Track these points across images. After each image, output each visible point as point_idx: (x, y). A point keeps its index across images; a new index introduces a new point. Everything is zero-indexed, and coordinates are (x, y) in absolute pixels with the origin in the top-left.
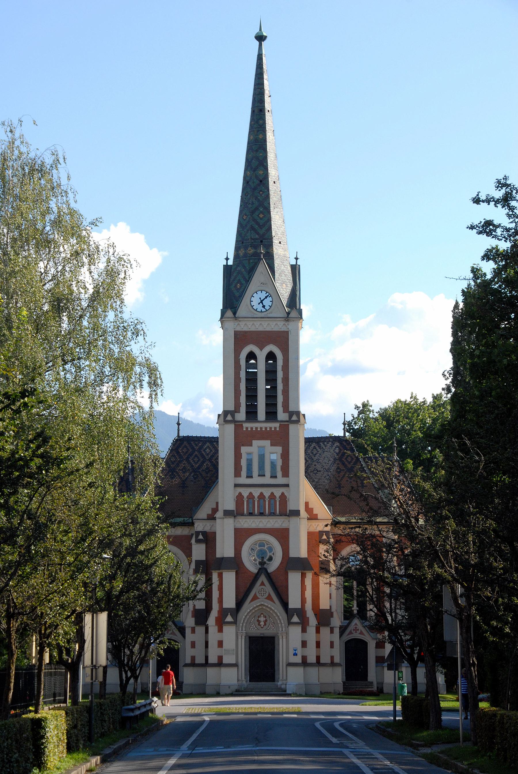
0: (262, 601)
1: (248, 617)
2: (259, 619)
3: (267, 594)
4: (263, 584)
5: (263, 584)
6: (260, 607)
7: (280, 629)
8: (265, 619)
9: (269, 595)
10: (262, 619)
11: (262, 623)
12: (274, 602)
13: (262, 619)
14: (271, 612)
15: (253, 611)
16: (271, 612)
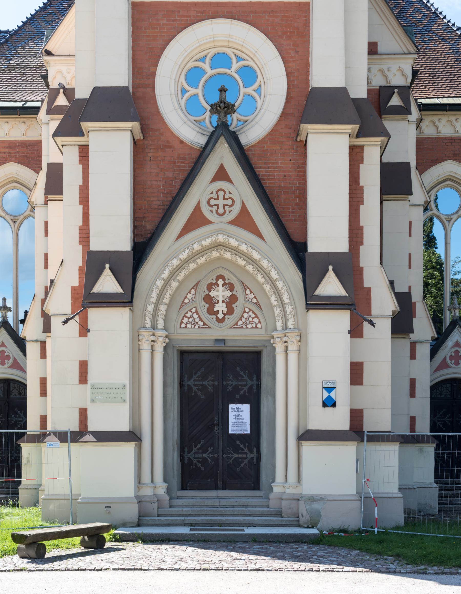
2: (212, 294)
8: (229, 293)
9: (244, 210)
10: (220, 293)
11: (221, 307)
13: (220, 293)
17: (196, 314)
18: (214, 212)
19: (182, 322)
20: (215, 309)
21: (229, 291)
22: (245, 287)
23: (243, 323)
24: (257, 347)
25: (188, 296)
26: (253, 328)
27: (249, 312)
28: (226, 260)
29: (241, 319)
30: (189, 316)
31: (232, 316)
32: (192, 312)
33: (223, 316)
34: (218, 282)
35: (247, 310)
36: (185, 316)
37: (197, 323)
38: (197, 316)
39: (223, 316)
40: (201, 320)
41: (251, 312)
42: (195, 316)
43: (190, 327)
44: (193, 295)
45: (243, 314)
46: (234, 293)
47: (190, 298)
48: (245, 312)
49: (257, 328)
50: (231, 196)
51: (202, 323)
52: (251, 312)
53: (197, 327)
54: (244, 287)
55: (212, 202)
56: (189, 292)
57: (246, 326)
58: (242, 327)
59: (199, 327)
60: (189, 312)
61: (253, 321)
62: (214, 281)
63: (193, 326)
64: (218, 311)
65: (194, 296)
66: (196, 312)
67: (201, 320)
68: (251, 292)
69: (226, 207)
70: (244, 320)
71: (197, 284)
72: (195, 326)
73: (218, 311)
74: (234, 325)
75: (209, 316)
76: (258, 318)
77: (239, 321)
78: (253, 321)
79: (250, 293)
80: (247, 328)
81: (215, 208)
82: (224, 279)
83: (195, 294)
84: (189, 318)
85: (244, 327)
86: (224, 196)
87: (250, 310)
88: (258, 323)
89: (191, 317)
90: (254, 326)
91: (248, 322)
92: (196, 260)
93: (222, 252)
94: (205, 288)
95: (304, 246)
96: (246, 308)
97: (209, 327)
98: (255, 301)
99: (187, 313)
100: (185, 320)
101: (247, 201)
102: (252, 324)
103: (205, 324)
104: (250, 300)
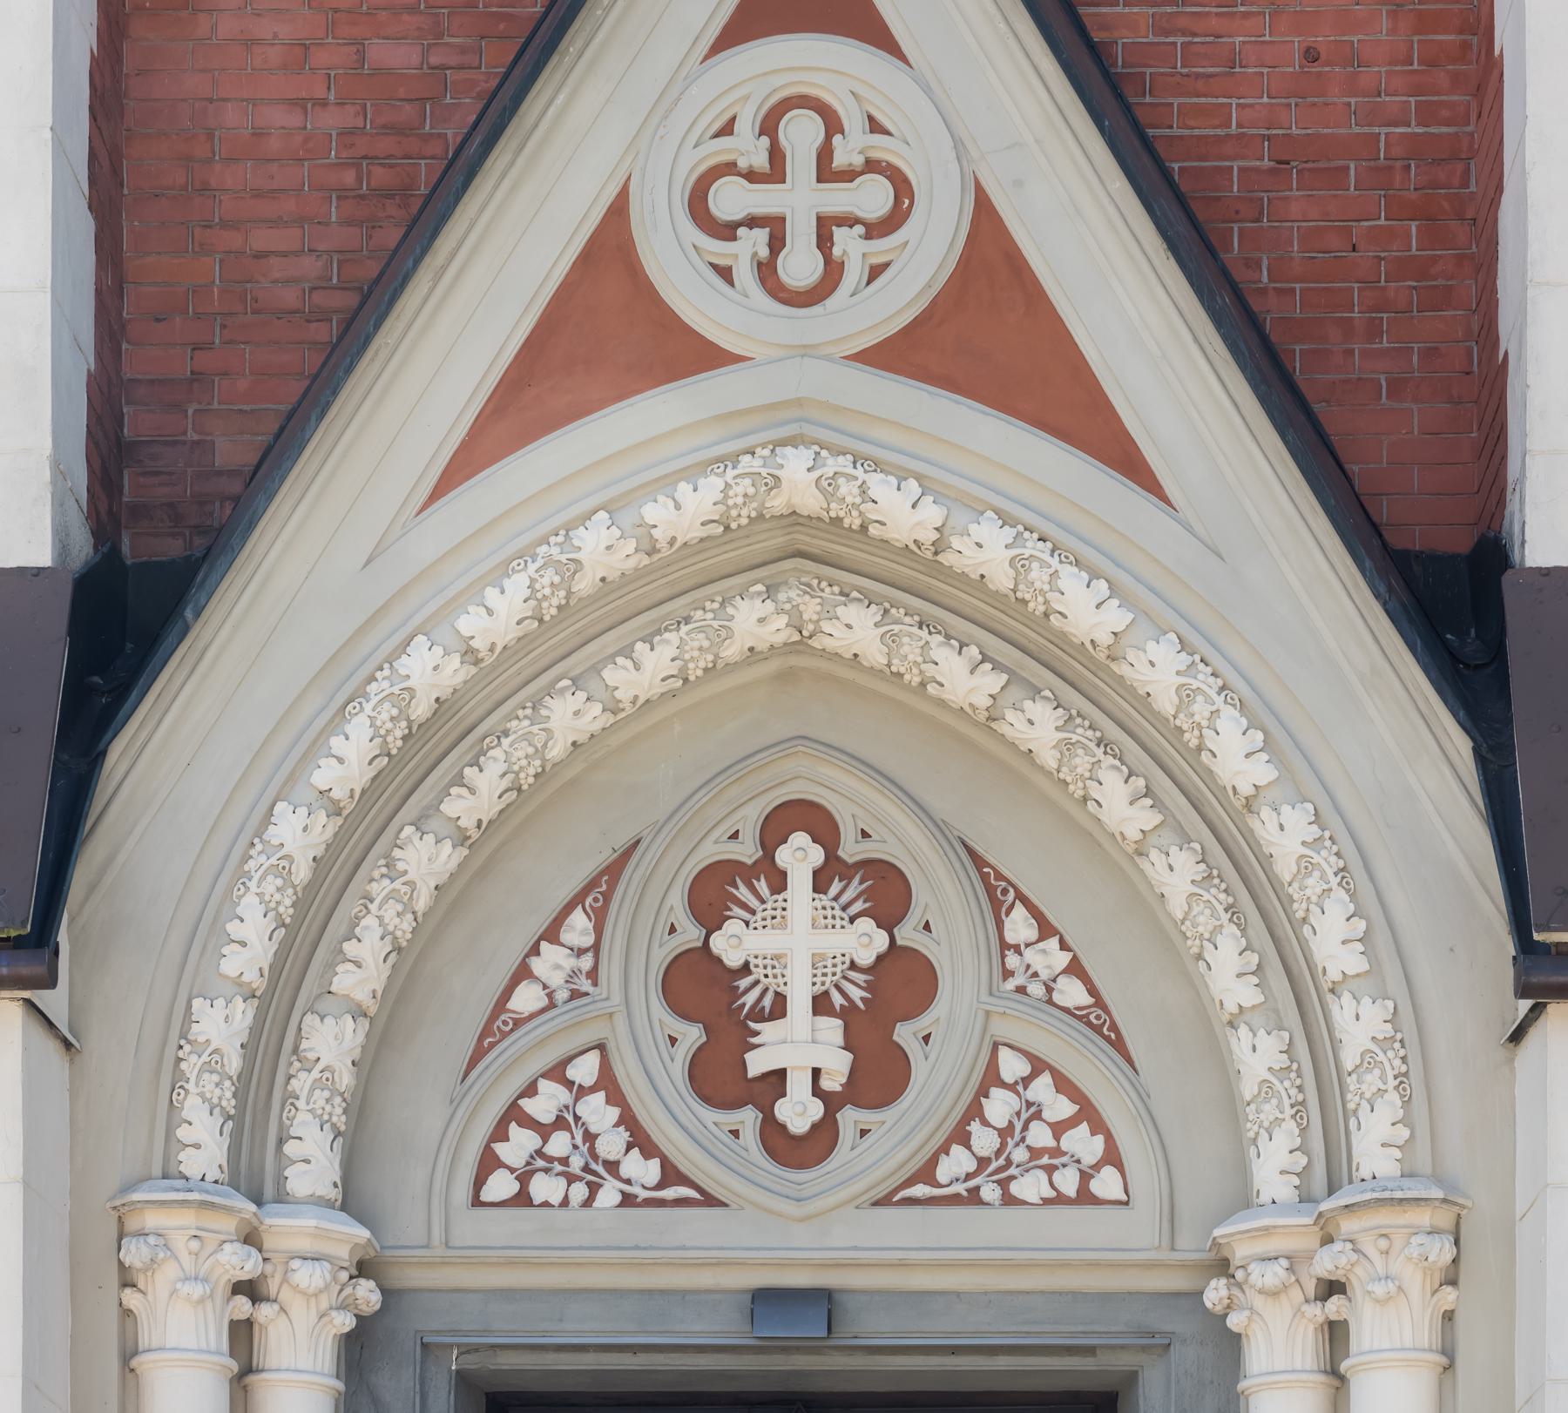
0: (794, 425)
1: (425, 860)
2: (731, 944)
3: (928, 252)
6: (754, 622)
7: (1275, 1164)
8: (866, 941)
9: (992, 262)
10: (799, 941)
11: (803, 1048)
12: (1127, 461)
13: (799, 941)
14: (1037, 726)
16: (1037, 726)
17: (600, 1097)
18: (745, 274)
19: (489, 1163)
20: (757, 1064)
21: (866, 924)
22: (997, 893)
23: (983, 1162)
24: (1090, 1350)
25: (536, 965)
26: (1059, 1199)
27: (1026, 1081)
28: (845, 677)
29: (961, 1136)
30: (547, 1118)
31: (889, 1114)
32: (569, 1084)
33: (817, 1109)
34: (783, 856)
35: (1012, 1066)
36: (514, 1114)
37: (613, 1167)
38: (614, 1113)
39: (817, 1109)
40: (641, 1142)
41: (1045, 1079)
42: (597, 1112)
43: (556, 1199)
44: (580, 952)
45: (983, 1092)
46: (907, 934)
47: (556, 980)
48: (992, 1077)
49: (1095, 1201)
50: (884, 149)
51: (655, 1164)
52: (1045, 1079)
53: (609, 1195)
54: (990, 890)
55: (730, 200)
56: (552, 934)
57: (1004, 1184)
58: (974, 1197)
59: (628, 1200)
60: (545, 1086)
61: (1057, 1152)
62: (747, 851)
63: (579, 1191)
64: (781, 1074)
65: (586, 962)
66: (607, 1083)
67: (641, 1142)
68: (1046, 929)
69: (839, 234)
70: (984, 1140)
71: (614, 870)
72: (594, 1189)
73: (781, 1074)
74: (909, 1183)
75: (710, 1115)
76: (1098, 1126)
77: (945, 1149)
79: (1033, 934)
80: (1009, 1200)
81: (754, 242)
82: (822, 826)
83: (596, 948)
84: (545, 1131)
85: (990, 1192)
86: (825, 154)
87: (1038, 1066)
88: (1097, 1167)
89: (560, 1123)
90: (1070, 1189)
91: (1020, 1155)
92: (596, 669)
93: (811, 608)
94: (677, 900)
95: (1491, 555)
96: (1005, 1055)
97: (709, 1201)
98: (1073, 993)
99: (531, 1090)
100: (518, 1146)
101: (1018, 183)
102: (1050, 1170)
103: (671, 1175)
104: (1036, 989)
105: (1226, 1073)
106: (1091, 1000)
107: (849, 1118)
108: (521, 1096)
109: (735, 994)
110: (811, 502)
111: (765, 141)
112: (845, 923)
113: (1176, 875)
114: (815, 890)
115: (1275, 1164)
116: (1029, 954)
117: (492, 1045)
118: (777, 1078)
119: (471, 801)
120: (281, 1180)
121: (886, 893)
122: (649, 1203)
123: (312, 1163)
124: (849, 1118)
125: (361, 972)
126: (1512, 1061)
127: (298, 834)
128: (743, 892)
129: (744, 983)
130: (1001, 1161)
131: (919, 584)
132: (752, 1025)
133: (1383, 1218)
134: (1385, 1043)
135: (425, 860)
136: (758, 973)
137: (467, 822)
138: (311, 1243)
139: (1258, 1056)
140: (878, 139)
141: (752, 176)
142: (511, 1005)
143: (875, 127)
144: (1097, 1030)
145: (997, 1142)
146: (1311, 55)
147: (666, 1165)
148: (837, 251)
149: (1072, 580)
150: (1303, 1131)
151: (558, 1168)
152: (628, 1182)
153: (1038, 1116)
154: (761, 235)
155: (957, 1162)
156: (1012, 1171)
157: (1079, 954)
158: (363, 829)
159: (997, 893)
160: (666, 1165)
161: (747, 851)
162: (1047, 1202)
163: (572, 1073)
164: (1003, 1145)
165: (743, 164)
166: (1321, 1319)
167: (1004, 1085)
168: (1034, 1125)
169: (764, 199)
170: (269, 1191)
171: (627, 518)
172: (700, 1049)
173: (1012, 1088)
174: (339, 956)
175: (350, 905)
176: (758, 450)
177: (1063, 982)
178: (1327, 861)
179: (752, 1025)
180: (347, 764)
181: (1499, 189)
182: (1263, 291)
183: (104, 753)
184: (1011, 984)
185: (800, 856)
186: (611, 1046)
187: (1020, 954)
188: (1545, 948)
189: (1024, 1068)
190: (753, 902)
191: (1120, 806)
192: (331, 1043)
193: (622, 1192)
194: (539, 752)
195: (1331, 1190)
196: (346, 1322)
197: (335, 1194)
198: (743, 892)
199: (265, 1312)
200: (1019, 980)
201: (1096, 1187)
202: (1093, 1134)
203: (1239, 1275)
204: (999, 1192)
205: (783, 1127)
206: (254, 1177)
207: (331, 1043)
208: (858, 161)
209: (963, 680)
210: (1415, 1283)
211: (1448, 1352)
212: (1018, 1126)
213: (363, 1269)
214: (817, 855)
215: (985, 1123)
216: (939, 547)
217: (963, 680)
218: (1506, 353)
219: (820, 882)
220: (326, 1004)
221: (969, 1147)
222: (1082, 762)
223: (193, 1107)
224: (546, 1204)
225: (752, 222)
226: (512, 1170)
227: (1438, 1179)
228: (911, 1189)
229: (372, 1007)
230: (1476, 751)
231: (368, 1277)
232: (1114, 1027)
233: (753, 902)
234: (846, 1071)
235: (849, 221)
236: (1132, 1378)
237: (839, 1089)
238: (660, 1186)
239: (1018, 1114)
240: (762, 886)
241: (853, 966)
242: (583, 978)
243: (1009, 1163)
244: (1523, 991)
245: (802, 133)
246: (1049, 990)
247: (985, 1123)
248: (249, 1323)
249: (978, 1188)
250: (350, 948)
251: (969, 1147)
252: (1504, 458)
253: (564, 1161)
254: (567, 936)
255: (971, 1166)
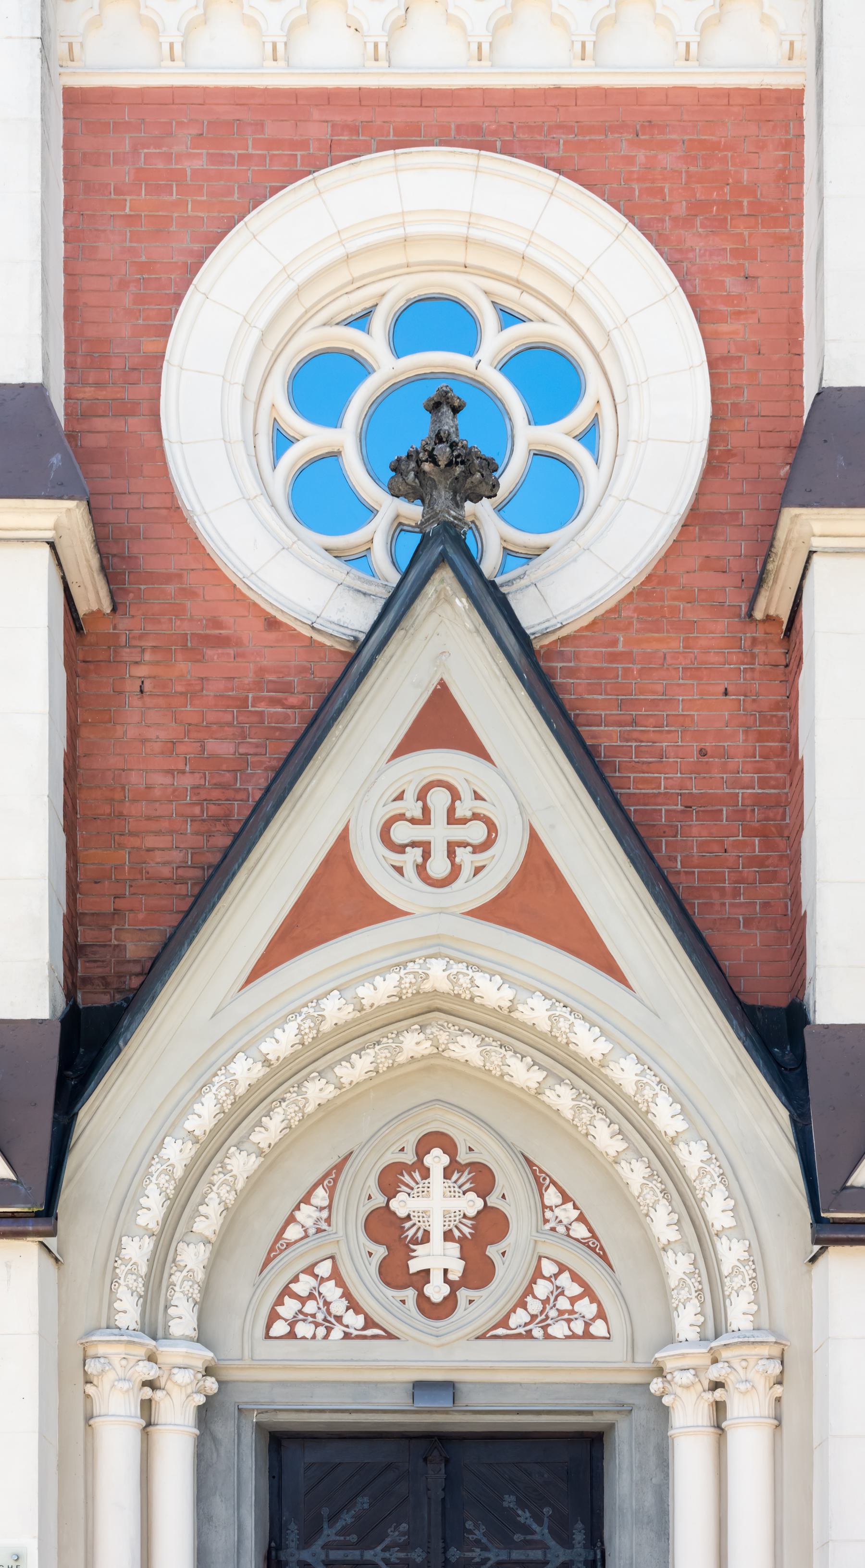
0: (436, 948)
1: (241, 1164)
2: (401, 1205)
4: (441, 723)
5: (441, 723)
6: (413, 1044)
7: (687, 1322)
8: (472, 1204)
9: (538, 865)
10: (437, 1204)
11: (438, 1258)
12: (608, 965)
13: (437, 1204)
14: (562, 1098)
15: (317, 1091)
16: (562, 1098)
17: (333, 1282)
18: (410, 871)
19: (274, 1316)
20: (415, 1266)
21: (472, 1195)
22: (540, 1180)
23: (533, 1317)
24: (590, 1413)
25: (298, 1215)
26: (574, 1336)
27: (556, 1276)
28: (461, 1071)
29: (522, 1304)
30: (304, 1293)
31: (484, 1292)
32: (316, 1276)
33: (446, 1290)
34: (428, 1160)
35: (548, 1268)
36: (287, 1291)
37: (339, 1319)
38: (339, 1291)
39: (446, 1290)
40: (354, 1306)
41: (566, 1275)
42: (331, 1291)
43: (309, 1335)
44: (322, 1209)
45: (533, 1281)
46: (493, 1200)
47: (309, 1223)
48: (538, 1274)
49: (592, 1337)
50: (481, 808)
52: (566, 1275)
53: (337, 1333)
54: (537, 1178)
55: (402, 833)
56: (306, 1200)
57: (545, 1328)
58: (529, 1335)
59: (347, 1336)
60: (302, 1277)
61: (572, 1312)
62: (409, 1158)
63: (321, 1331)
64: (427, 1272)
65: (325, 1214)
66: (336, 1276)
67: (354, 1306)
68: (566, 1198)
69: (459, 851)
70: (534, 1306)
71: (339, 1167)
72: (329, 1330)
73: (427, 1272)
74: (495, 1327)
75: (390, 1292)
76: (594, 1299)
77: (513, 1310)
78: (572, 1312)
79: (559, 1201)
80: (547, 1337)
81: (415, 854)
83: (330, 1207)
84: (303, 1300)
85: (537, 1332)
86: (451, 810)
87: (562, 1268)
88: (593, 1320)
89: (311, 1296)
90: (580, 1333)
91: (553, 1313)
92: (331, 1067)
93: (443, 1037)
96: (544, 1262)
97: (390, 1336)
98: (580, 1231)
99: (296, 1279)
100: (289, 1308)
101: (552, 827)
102: (569, 1321)
103: (370, 1323)
104: (561, 1229)
105: (661, 1274)
106: (590, 1235)
107: (463, 1294)
108: (290, 1282)
109: (403, 1230)
110: (444, 986)
111: (420, 803)
112: (461, 1195)
113: (634, 1174)
114: (445, 1177)
115: (687, 1322)
116: (557, 1211)
117: (275, 1256)
118: (425, 1274)
119: (265, 1134)
120: (166, 1327)
121: (482, 1179)
122: (358, 1337)
123: (183, 1318)
124: (463, 1294)
125: (208, 1220)
126: (810, 1271)
127: (177, 1153)
128: (407, 1178)
129: (407, 1225)
130: (543, 1317)
131: (501, 1027)
132: (412, 1246)
133: (745, 1351)
134: (744, 1262)
135: (241, 1164)
136: (415, 1220)
137: (264, 1145)
138: (182, 1357)
139: (678, 1266)
140: (479, 803)
141: (413, 821)
142: (285, 1236)
143: (477, 797)
144: (593, 1250)
145: (541, 1307)
146: (703, 753)
147: (367, 1318)
148: (458, 860)
149: (581, 1027)
150: (702, 1304)
151: (310, 1319)
152: (347, 1326)
153: (562, 1293)
154: (418, 851)
155: (519, 1318)
156: (549, 1321)
157: (584, 1212)
158: (209, 1153)
159: (540, 1180)
160: (367, 1318)
161: (409, 1158)
162: (567, 1337)
163: (317, 1270)
164: (544, 1308)
165: (408, 815)
166: (712, 1400)
167: (544, 1278)
168: (560, 1298)
169: (419, 833)
170: (160, 1333)
171: (349, 994)
172: (385, 1258)
173: (549, 1279)
174: (196, 1213)
175: (202, 1187)
176: (417, 960)
177: (575, 1225)
178: (714, 1170)
179: (412, 1246)
180: (203, 1116)
181: (801, 827)
182: (678, 873)
183: (77, 1114)
184: (548, 1226)
185: (436, 1160)
186: (338, 1257)
187: (552, 1211)
188: (827, 1221)
189: (555, 1269)
190: (412, 1184)
191: (605, 1138)
192: (192, 1257)
193: (344, 1332)
194: (301, 1110)
195: (717, 1336)
196: (201, 1400)
197: (194, 1334)
198: (407, 1178)
199: (159, 1394)
200: (552, 1224)
201: (593, 1330)
202: (591, 1302)
203: (669, 1377)
204: (542, 1332)
205: (428, 1299)
206: (153, 1328)
207: (192, 1257)
208: (469, 814)
209: (523, 1074)
210: (761, 1384)
211: (778, 1418)
212: (552, 1299)
213: (208, 1371)
214: (446, 1160)
215: (535, 1297)
216: (511, 1010)
217: (523, 1074)
218: (805, 912)
219: (447, 1174)
220: (190, 1237)
221: (526, 1309)
222: (586, 1117)
223: (122, 1292)
224: (304, 1338)
225: (414, 844)
226: (286, 1320)
227: (772, 1331)
228: (497, 1330)
229: (213, 1238)
230: (791, 1117)
231: (211, 1376)
232: (602, 1248)
233: (412, 1184)
234: (461, 1270)
235: (465, 845)
236: (612, 1426)
237: (458, 1279)
238: (364, 1328)
239: (552, 1293)
240: (417, 1175)
241: (465, 1216)
242: (323, 1222)
243: (547, 1317)
244: (816, 1241)
245: (439, 800)
246: (568, 1229)
247: (535, 1297)
248: (150, 1400)
249: (531, 1330)
250: (202, 1209)
251: (526, 1309)
252: (804, 964)
253: (313, 1316)
254: (313, 1201)
255: (527, 1319)
